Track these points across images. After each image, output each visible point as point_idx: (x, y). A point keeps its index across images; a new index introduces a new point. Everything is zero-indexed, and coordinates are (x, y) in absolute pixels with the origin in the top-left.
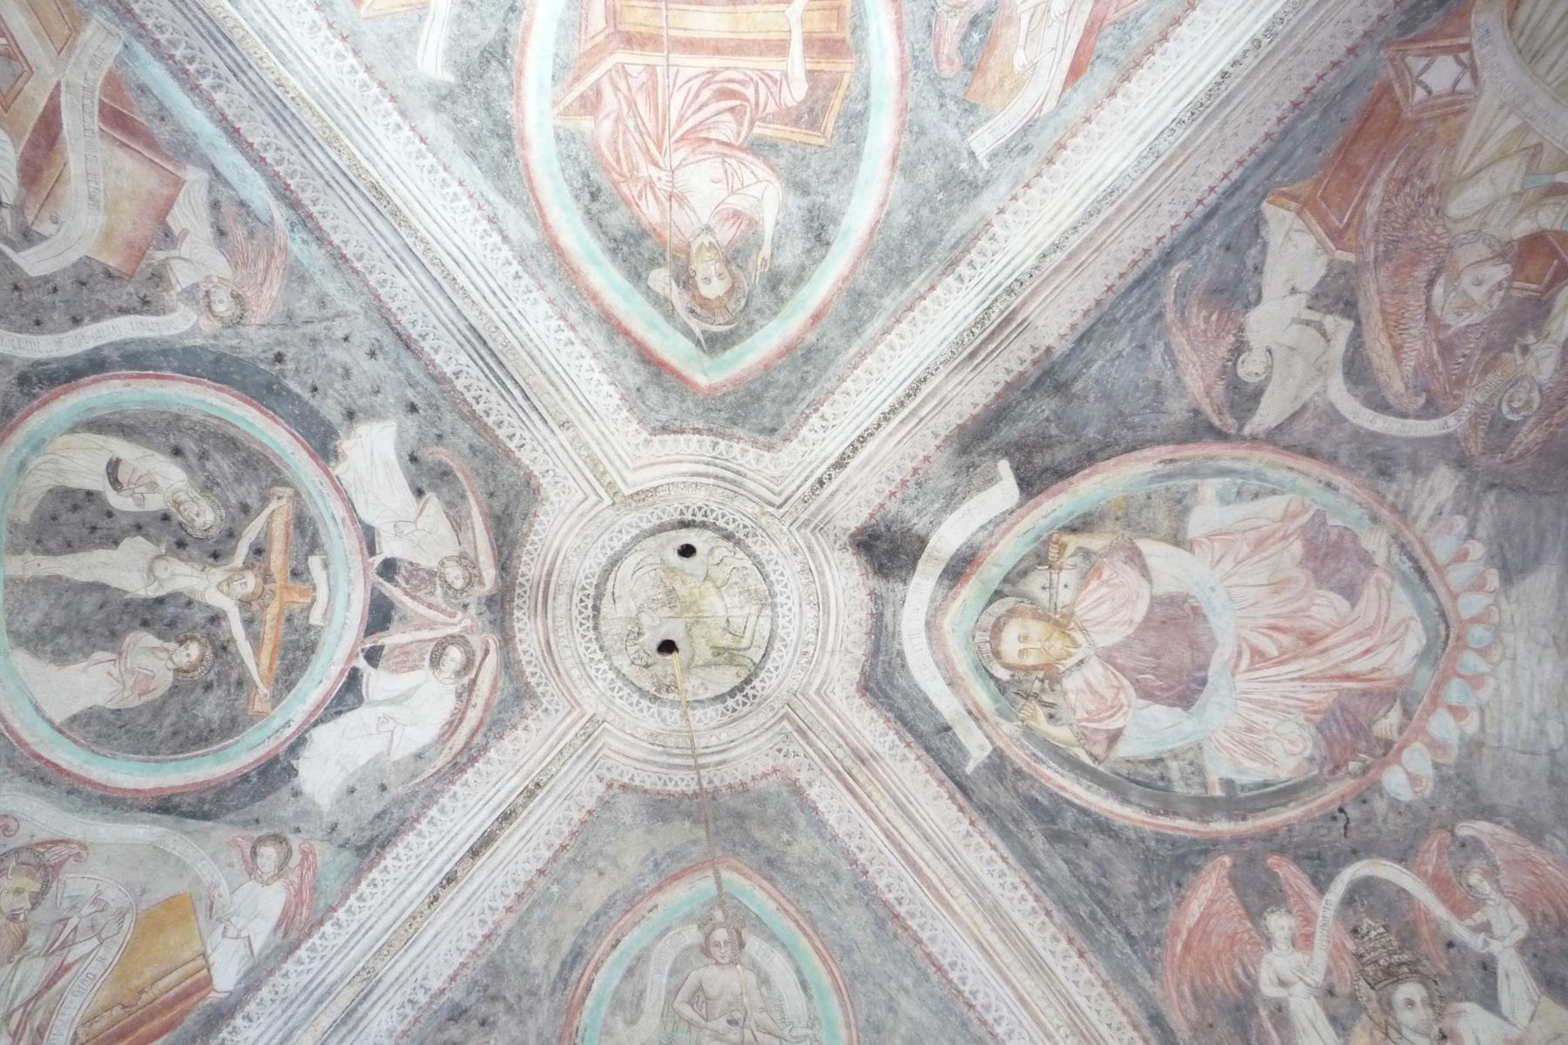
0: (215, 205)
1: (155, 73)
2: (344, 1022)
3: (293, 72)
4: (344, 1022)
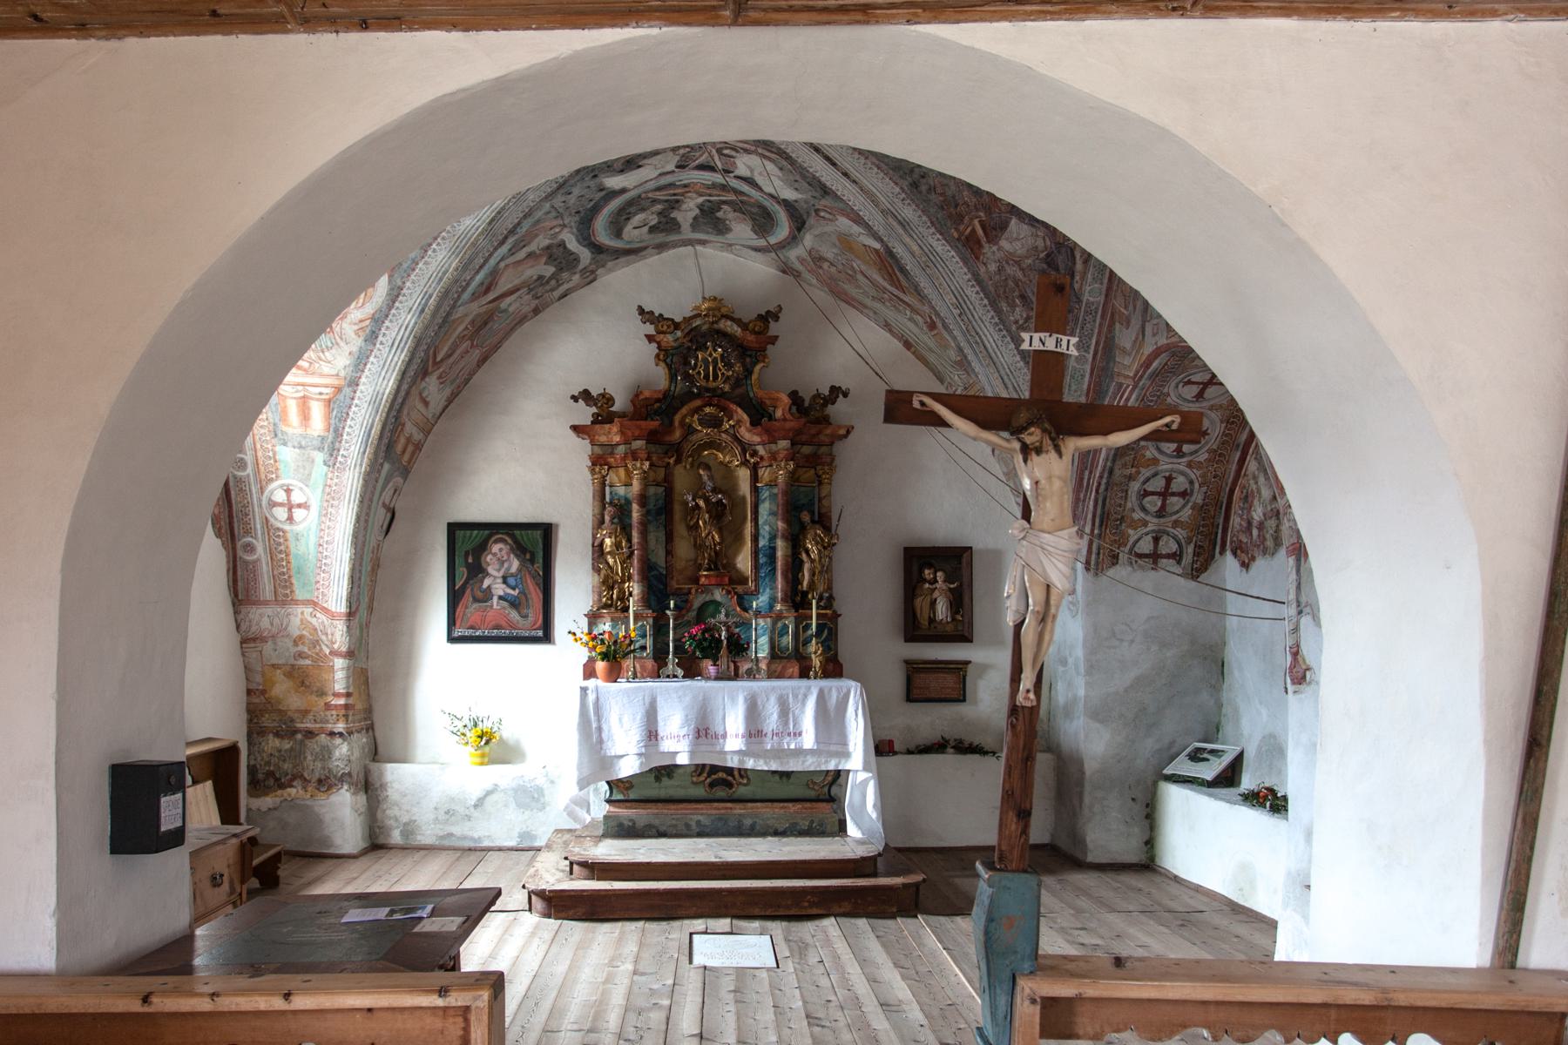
0: (513, 254)
1: (466, 296)
2: (904, 226)
3: (450, 266)
4: (904, 226)
